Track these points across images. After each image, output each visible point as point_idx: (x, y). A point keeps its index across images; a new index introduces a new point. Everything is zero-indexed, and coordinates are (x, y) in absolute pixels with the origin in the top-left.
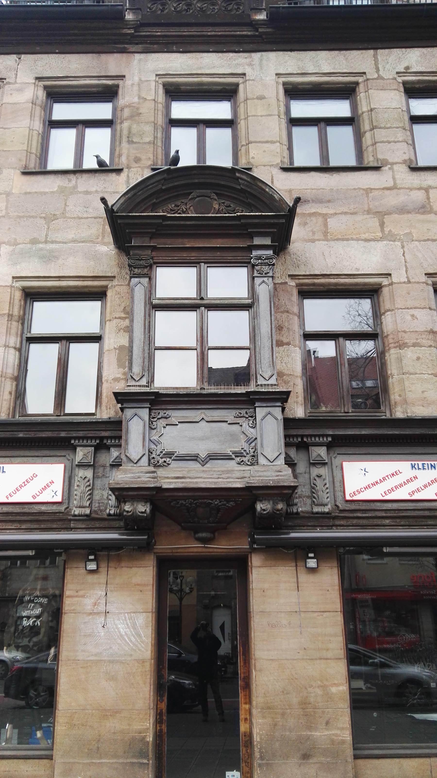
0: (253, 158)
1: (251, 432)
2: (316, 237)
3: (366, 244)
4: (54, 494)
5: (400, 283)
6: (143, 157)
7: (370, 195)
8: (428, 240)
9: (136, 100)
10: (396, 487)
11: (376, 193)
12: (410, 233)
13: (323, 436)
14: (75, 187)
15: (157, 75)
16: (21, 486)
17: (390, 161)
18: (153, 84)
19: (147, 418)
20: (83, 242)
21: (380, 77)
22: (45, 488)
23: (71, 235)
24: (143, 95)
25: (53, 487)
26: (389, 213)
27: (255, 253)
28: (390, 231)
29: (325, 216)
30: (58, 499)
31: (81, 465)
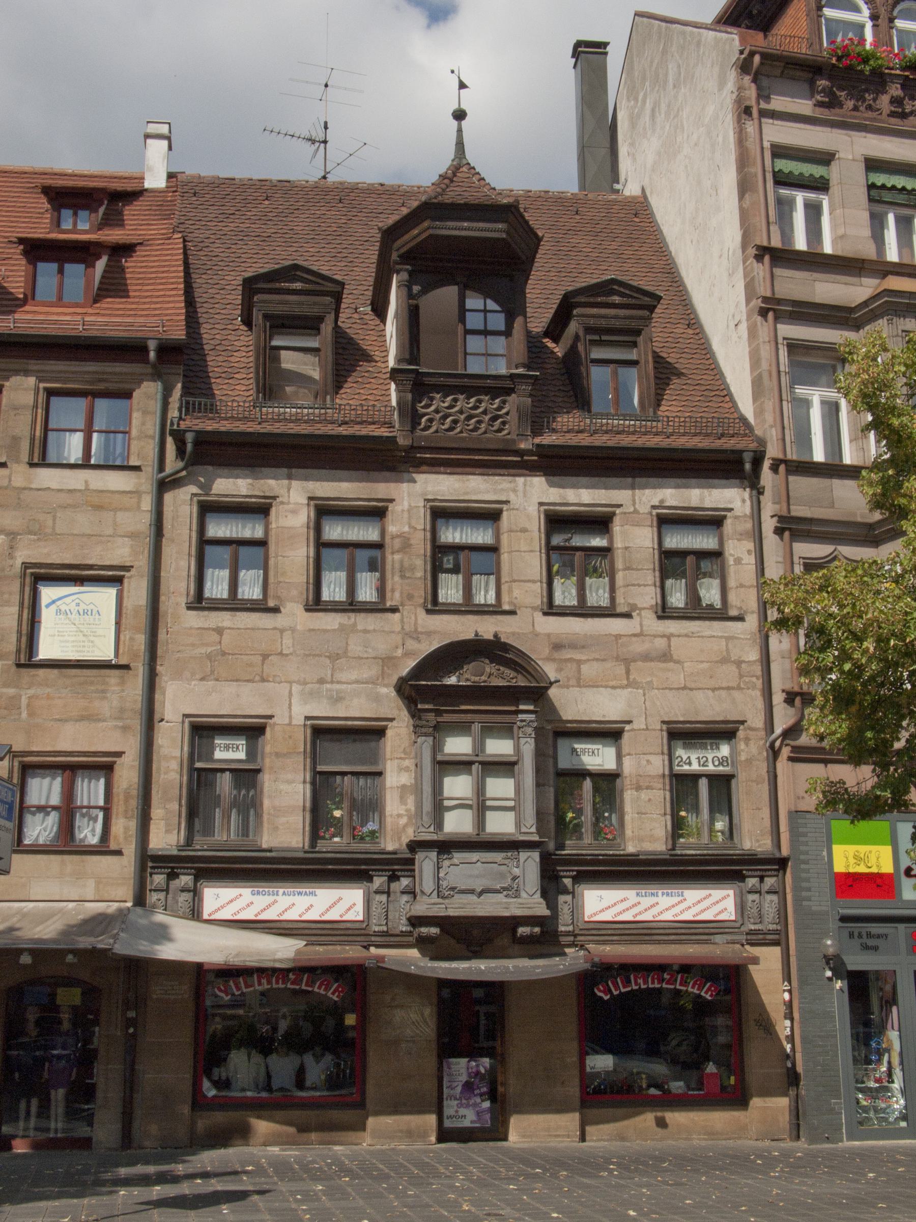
0: (516, 598)
1: (516, 871)
2: (571, 683)
3: (613, 691)
4: (357, 914)
5: (640, 730)
6: (416, 594)
7: (620, 641)
8: (666, 688)
9: (406, 529)
10: (624, 911)
11: (624, 639)
12: (651, 681)
13: (570, 871)
15: (425, 500)
16: (330, 907)
17: (639, 606)
18: (422, 510)
19: (435, 860)
20: (363, 683)
21: (636, 511)
22: (349, 909)
23: (354, 675)
24: (414, 523)
25: (355, 908)
26: (635, 661)
28: (634, 679)
29: (579, 662)
30: (361, 918)
31: (377, 892)
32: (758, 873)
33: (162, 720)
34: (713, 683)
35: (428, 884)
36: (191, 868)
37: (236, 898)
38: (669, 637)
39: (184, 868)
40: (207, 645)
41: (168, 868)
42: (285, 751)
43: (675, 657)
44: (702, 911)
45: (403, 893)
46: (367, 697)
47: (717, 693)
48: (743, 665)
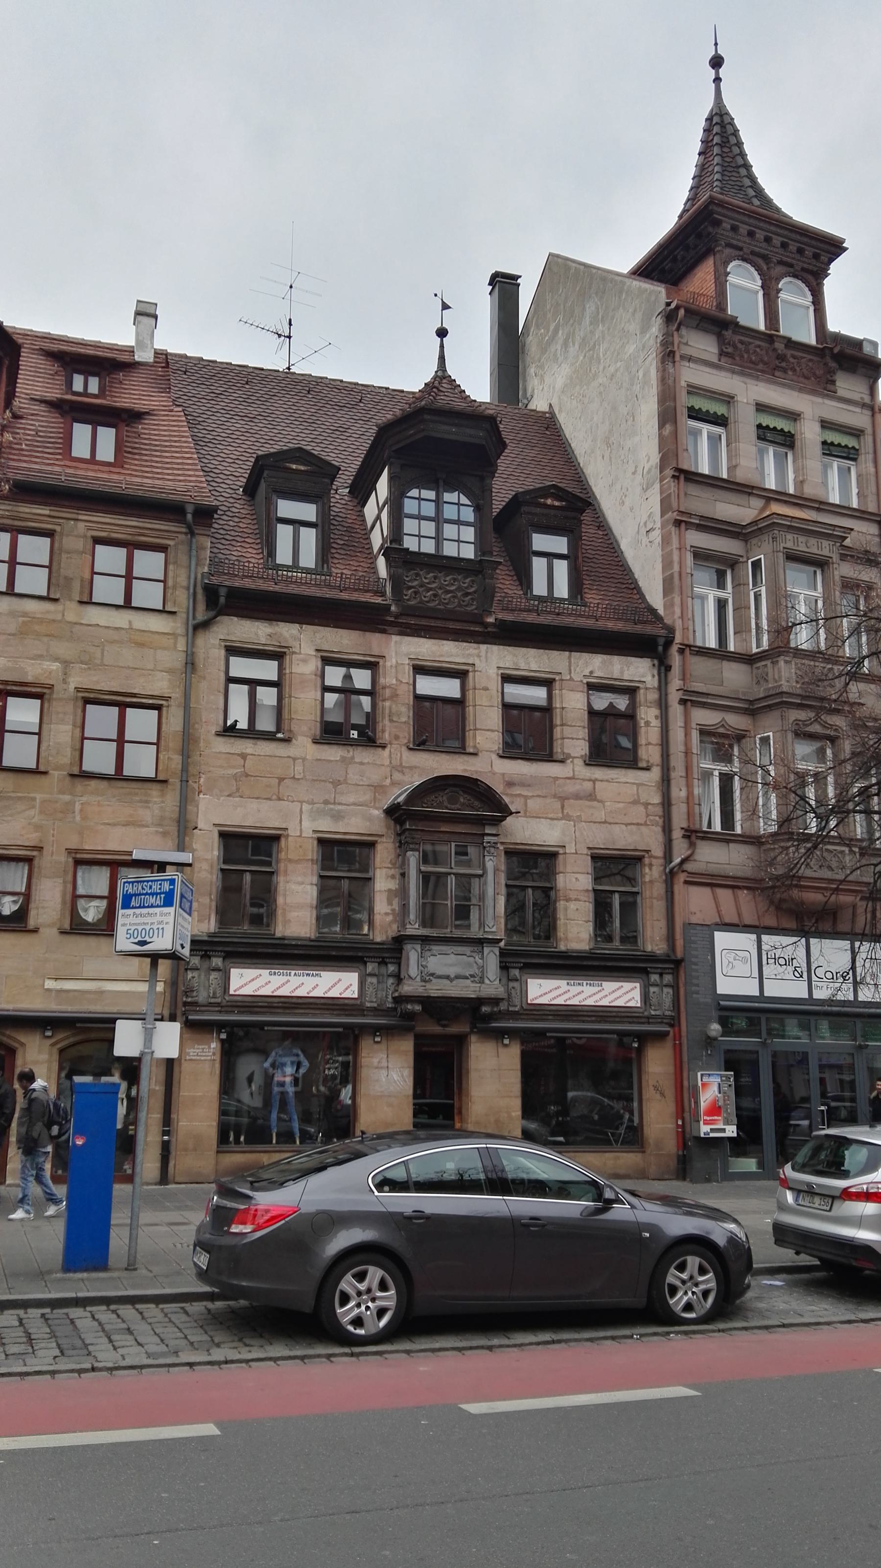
4: (353, 992)
6: (401, 735)
9: (394, 681)
11: (561, 781)
14: (353, 758)
17: (572, 755)
19: (419, 950)
21: (571, 679)
22: (347, 989)
23: (351, 799)
24: (400, 678)
25: (352, 988)
26: (568, 799)
27: (486, 839)
29: (526, 798)
30: (356, 996)
31: (370, 975)
32: (659, 971)
33: (196, 828)
34: (627, 820)
35: (413, 971)
36: (221, 951)
37: (257, 977)
38: (594, 781)
39: (216, 951)
40: (234, 767)
41: (202, 951)
42: (297, 858)
43: (598, 797)
44: (616, 999)
45: (389, 976)
46: (362, 819)
47: (629, 827)
48: (650, 807)
